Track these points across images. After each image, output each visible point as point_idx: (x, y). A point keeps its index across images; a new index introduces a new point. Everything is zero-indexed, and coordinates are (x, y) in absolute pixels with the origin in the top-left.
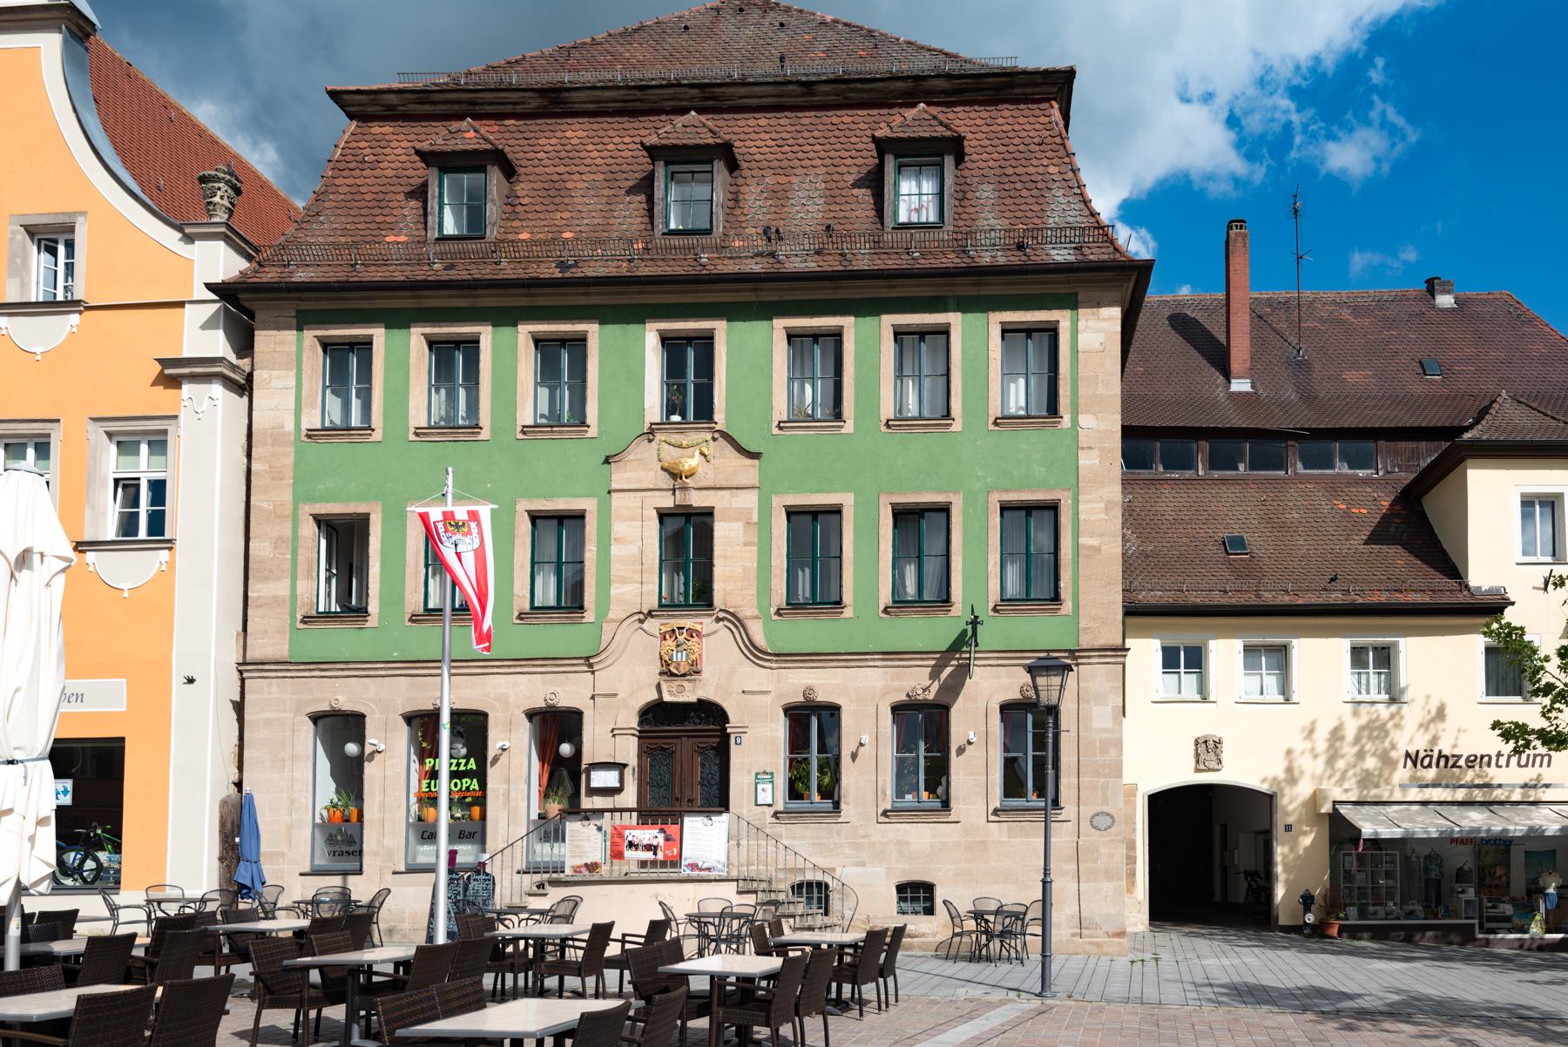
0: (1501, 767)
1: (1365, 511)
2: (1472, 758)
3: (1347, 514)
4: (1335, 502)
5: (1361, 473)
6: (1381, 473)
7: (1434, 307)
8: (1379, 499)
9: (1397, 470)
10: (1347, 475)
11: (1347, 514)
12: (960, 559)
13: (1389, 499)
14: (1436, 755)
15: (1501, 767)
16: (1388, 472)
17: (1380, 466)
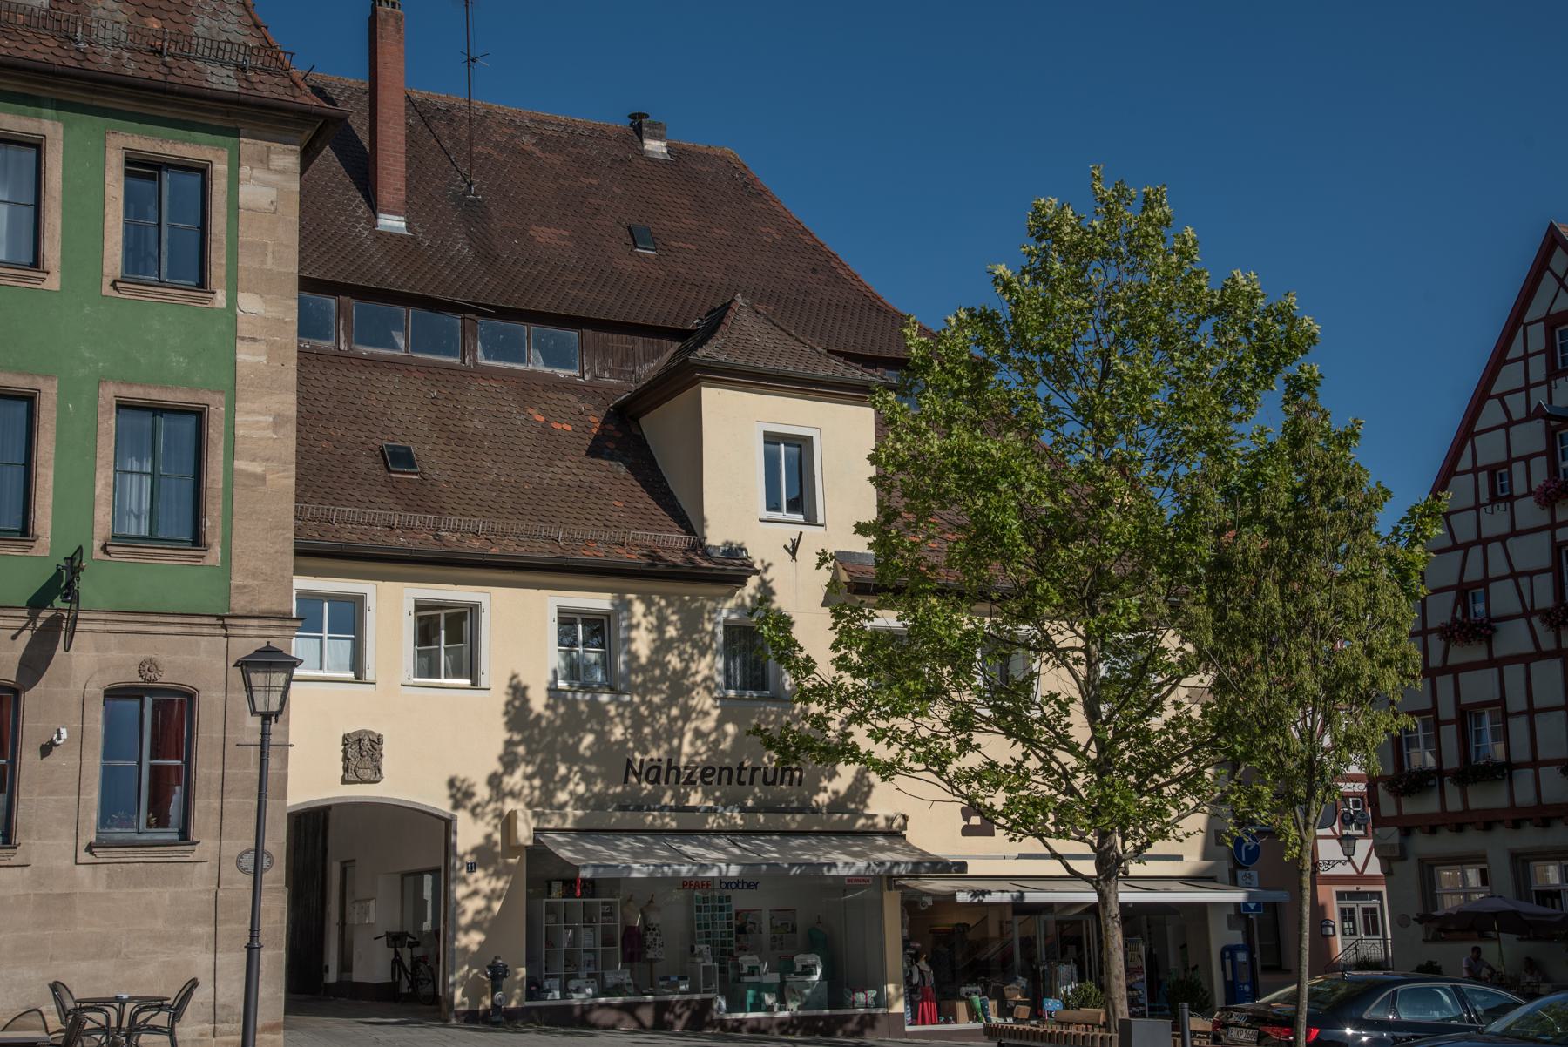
0: (743, 784)
1: (569, 428)
2: (709, 772)
3: (546, 429)
4: (530, 410)
5: (561, 373)
6: (587, 377)
7: (642, 152)
8: (586, 413)
9: (607, 375)
10: (543, 374)
11: (546, 429)
12: (51, 473)
13: (598, 413)
14: (664, 766)
15: (743, 784)
16: (596, 377)
17: (586, 368)
